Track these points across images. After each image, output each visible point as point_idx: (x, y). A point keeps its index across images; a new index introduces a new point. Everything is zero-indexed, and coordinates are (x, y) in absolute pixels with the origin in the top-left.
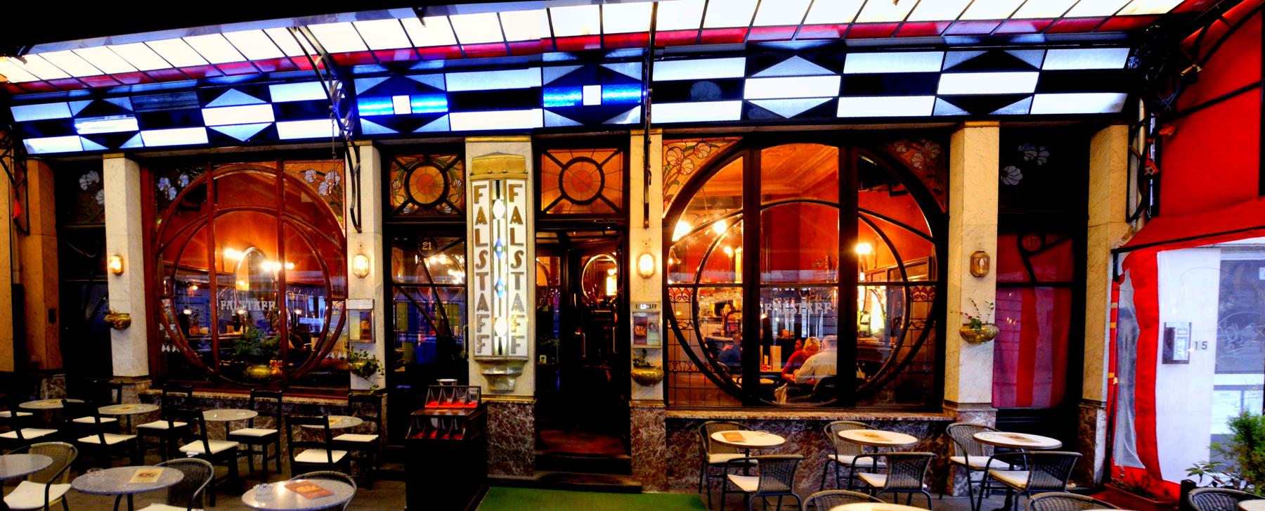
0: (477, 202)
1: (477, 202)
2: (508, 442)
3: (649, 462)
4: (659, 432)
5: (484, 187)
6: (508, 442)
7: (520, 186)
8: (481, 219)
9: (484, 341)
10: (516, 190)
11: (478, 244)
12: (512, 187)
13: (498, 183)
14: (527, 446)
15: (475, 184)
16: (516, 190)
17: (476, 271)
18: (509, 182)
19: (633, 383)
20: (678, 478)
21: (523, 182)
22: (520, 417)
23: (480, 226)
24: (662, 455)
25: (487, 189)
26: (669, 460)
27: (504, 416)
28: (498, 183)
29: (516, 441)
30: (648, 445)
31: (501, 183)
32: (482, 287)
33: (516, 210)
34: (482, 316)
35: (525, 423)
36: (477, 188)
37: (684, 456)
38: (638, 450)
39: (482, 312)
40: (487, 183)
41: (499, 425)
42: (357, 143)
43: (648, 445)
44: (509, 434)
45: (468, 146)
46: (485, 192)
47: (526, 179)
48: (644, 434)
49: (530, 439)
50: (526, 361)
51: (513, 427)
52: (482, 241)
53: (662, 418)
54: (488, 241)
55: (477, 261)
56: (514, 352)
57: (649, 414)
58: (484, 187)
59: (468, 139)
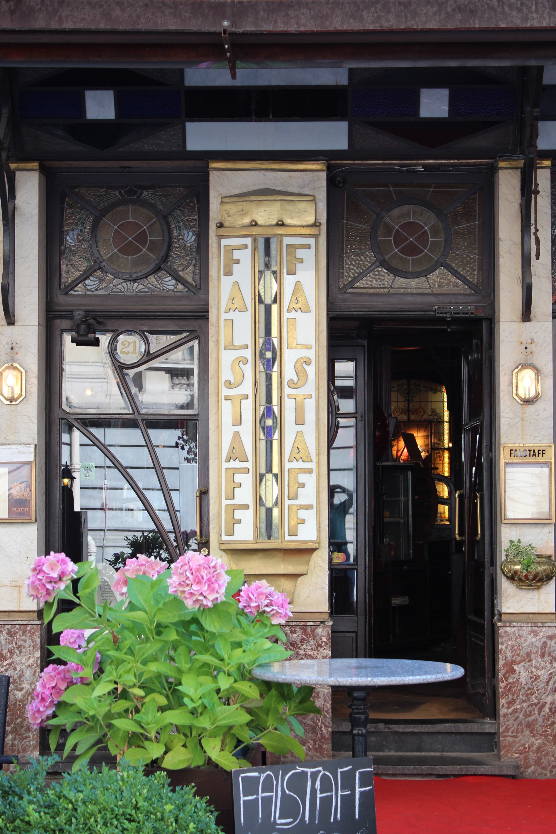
0: (229, 273)
1: (229, 273)
3: (529, 725)
7: (308, 247)
9: (238, 514)
10: (300, 253)
11: (231, 346)
13: (267, 242)
15: (224, 242)
17: (225, 392)
18: (287, 241)
21: (312, 241)
25: (248, 252)
28: (267, 242)
30: (529, 693)
33: (298, 287)
34: (236, 471)
36: (230, 250)
38: (510, 703)
39: (236, 464)
40: (248, 241)
42: (13, 166)
43: (529, 693)
45: (214, 177)
46: (245, 256)
47: (316, 236)
48: (522, 674)
50: (311, 551)
54: (249, 341)
56: (293, 533)
57: (531, 639)
59: (214, 165)
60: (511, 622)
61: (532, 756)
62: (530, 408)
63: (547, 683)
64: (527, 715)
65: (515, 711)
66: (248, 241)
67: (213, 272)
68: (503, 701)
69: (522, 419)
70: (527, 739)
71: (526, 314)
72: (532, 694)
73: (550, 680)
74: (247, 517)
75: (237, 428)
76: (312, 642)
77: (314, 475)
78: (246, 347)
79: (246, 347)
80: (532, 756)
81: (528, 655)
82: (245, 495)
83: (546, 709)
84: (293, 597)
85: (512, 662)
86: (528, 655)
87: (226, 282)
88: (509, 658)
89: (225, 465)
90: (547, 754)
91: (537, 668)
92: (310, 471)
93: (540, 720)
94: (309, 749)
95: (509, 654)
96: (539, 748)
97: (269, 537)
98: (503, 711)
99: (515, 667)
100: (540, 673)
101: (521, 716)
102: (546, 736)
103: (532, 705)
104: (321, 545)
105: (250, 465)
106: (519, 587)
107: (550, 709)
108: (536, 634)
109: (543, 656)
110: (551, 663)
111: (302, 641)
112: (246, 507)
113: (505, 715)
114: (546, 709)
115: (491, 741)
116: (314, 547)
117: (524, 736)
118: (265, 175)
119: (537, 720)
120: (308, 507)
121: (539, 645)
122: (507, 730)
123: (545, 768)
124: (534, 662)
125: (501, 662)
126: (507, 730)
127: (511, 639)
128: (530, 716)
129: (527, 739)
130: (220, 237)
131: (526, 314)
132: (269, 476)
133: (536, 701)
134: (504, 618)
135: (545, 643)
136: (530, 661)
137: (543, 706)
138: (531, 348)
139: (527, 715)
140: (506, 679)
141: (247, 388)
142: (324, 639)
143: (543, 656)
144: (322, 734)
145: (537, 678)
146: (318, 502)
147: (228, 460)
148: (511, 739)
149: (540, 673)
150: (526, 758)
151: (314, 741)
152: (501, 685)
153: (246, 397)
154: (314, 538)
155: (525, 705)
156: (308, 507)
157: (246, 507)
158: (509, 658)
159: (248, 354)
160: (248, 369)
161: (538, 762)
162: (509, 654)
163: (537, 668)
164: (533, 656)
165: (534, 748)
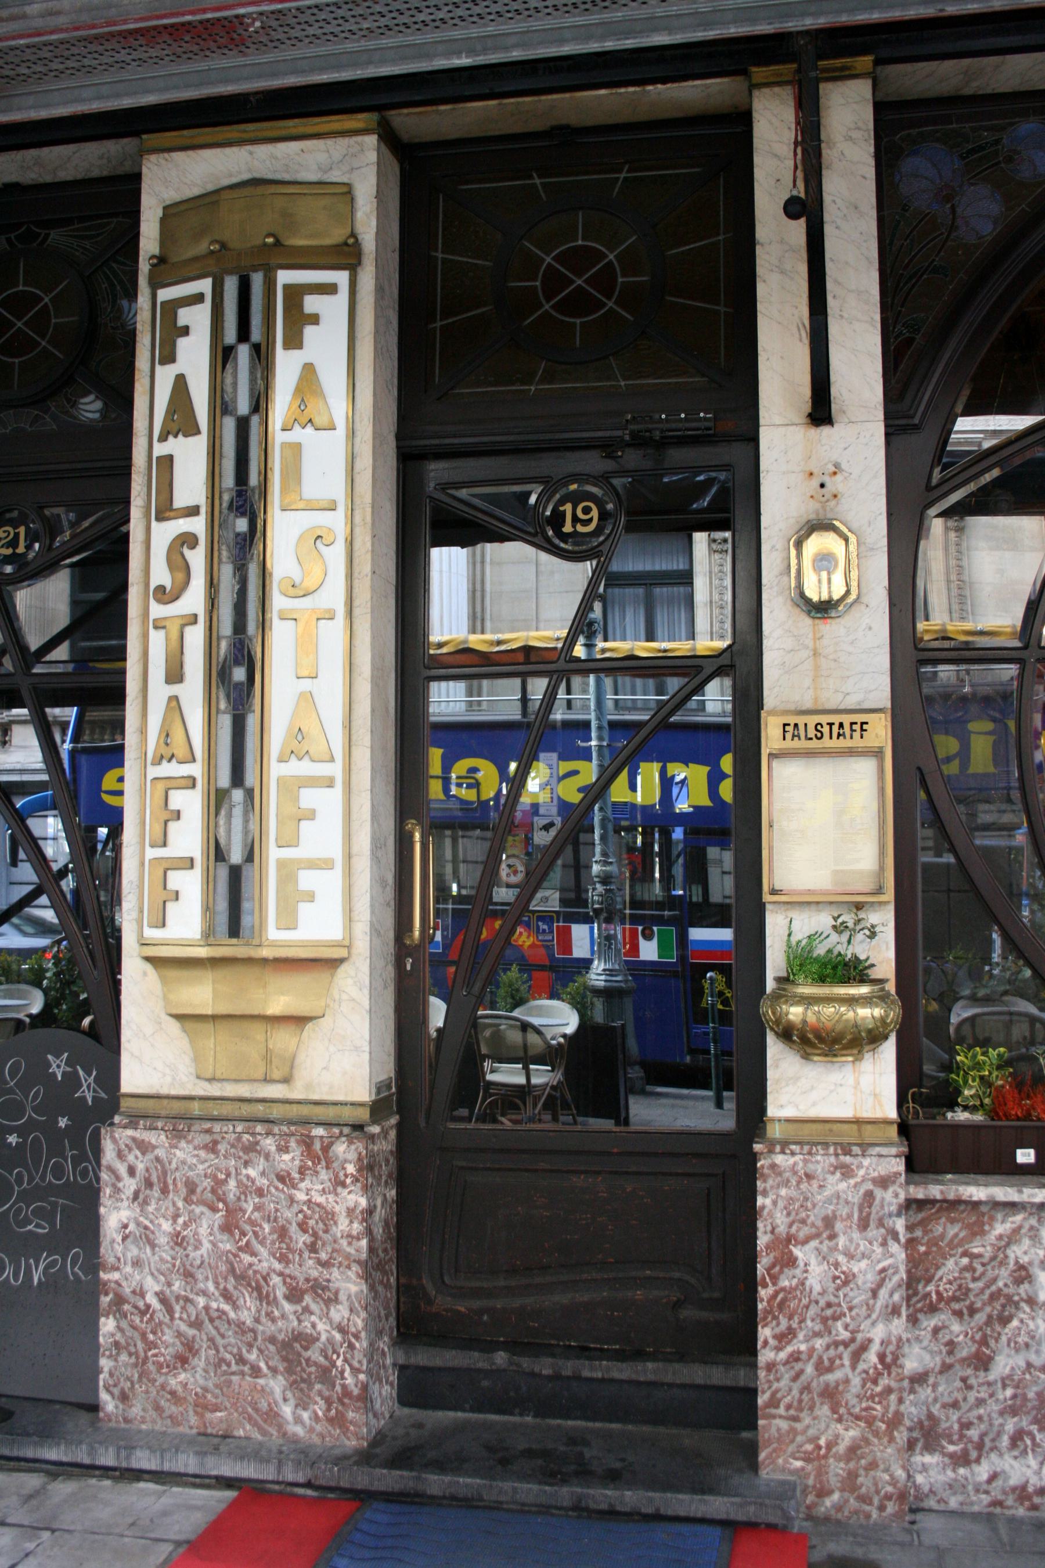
0: (169, 358)
2: (264, 1297)
3: (831, 1395)
4: (876, 1259)
5: (199, 298)
6: (264, 1297)
7: (330, 289)
8: (180, 419)
11: (165, 511)
12: (295, 294)
14: (339, 1313)
15: (165, 294)
16: (312, 303)
17: (157, 611)
18: (285, 277)
19: (774, 1047)
20: (962, 1460)
21: (341, 278)
22: (312, 1189)
23: (179, 447)
24: (889, 1361)
26: (919, 1379)
27: (245, 1190)
29: (294, 1295)
31: (257, 280)
32: (175, 675)
35: (328, 1217)
36: (172, 307)
37: (982, 1362)
38: (784, 1338)
41: (227, 1228)
44: (265, 1261)
48: (812, 1267)
49: (350, 1284)
50: (333, 964)
51: (283, 1233)
52: (180, 501)
53: (892, 1197)
55: (161, 575)
56: (289, 921)
57: (836, 1184)
58: (199, 298)
60: (785, 1144)
61: (837, 1469)
62: (832, 629)
63: (875, 1293)
64: (822, 1368)
65: (795, 1357)
66: (205, 286)
67: (142, 362)
68: (765, 1333)
69: (816, 653)
70: (825, 1427)
71: (821, 411)
72: (836, 1318)
73: (880, 1284)
74: (190, 885)
75: (175, 689)
76: (324, 1175)
77: (337, 793)
78: (193, 511)
79: (193, 511)
80: (837, 1469)
81: (829, 1222)
82: (188, 838)
83: (871, 1357)
84: (292, 1067)
85: (789, 1239)
86: (829, 1222)
87: (166, 376)
88: (782, 1229)
89: (153, 772)
90: (873, 1465)
91: (851, 1257)
92: (330, 783)
93: (856, 1381)
94: (316, 1418)
95: (781, 1220)
96: (853, 1450)
97: (234, 929)
98: (765, 1356)
99: (797, 1252)
100: (857, 1267)
101: (810, 1369)
102: (870, 1422)
103: (836, 1344)
104: (354, 951)
105: (196, 770)
106: (806, 1057)
107: (882, 1357)
108: (847, 1172)
109: (864, 1225)
110: (884, 1244)
111: (302, 1170)
112: (190, 863)
113: (771, 1367)
114: (871, 1357)
115: (737, 1413)
116: (335, 956)
117: (814, 1419)
118: (251, 153)
119: (847, 1381)
120: (326, 864)
121: (856, 1198)
122: (774, 1403)
123: (865, 1499)
124: (842, 1241)
125: (763, 1240)
126: (774, 1403)
127: (787, 1183)
128: (830, 1369)
129: (825, 1427)
130: (156, 284)
131: (821, 411)
132: (238, 795)
133: (845, 1335)
134: (775, 1131)
135: (869, 1195)
136: (832, 1237)
137: (864, 1347)
138: (835, 484)
139: (822, 1368)
140: (775, 1279)
141: (194, 599)
142: (351, 1169)
143: (864, 1225)
144: (344, 1387)
145: (848, 1279)
146: (348, 856)
147: (159, 760)
148: (784, 1425)
149: (857, 1267)
150: (820, 1472)
151: (329, 1402)
152: (763, 1293)
153: (194, 619)
154: (334, 931)
155: (819, 1343)
156: (326, 864)
157: (190, 863)
158: (782, 1229)
159: (198, 525)
160: (197, 559)
161: (850, 1482)
162: (781, 1220)
163: (851, 1257)
164: (839, 1226)
165: (841, 1448)
